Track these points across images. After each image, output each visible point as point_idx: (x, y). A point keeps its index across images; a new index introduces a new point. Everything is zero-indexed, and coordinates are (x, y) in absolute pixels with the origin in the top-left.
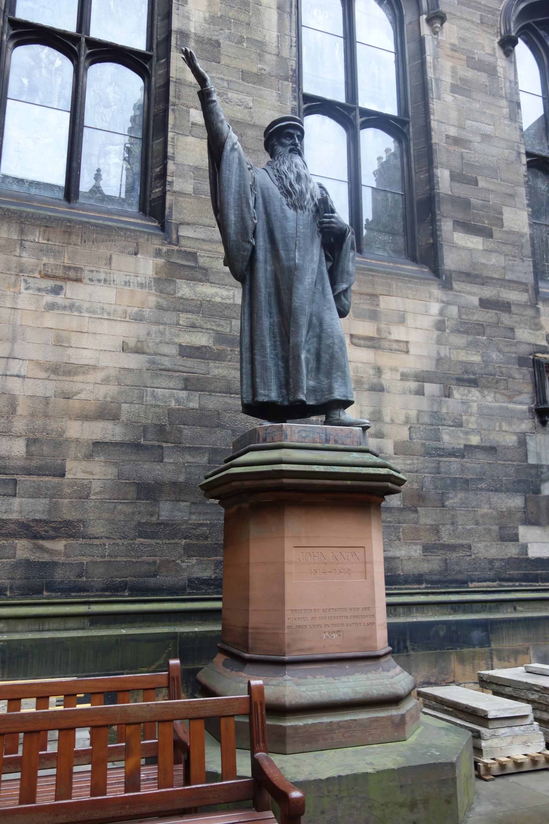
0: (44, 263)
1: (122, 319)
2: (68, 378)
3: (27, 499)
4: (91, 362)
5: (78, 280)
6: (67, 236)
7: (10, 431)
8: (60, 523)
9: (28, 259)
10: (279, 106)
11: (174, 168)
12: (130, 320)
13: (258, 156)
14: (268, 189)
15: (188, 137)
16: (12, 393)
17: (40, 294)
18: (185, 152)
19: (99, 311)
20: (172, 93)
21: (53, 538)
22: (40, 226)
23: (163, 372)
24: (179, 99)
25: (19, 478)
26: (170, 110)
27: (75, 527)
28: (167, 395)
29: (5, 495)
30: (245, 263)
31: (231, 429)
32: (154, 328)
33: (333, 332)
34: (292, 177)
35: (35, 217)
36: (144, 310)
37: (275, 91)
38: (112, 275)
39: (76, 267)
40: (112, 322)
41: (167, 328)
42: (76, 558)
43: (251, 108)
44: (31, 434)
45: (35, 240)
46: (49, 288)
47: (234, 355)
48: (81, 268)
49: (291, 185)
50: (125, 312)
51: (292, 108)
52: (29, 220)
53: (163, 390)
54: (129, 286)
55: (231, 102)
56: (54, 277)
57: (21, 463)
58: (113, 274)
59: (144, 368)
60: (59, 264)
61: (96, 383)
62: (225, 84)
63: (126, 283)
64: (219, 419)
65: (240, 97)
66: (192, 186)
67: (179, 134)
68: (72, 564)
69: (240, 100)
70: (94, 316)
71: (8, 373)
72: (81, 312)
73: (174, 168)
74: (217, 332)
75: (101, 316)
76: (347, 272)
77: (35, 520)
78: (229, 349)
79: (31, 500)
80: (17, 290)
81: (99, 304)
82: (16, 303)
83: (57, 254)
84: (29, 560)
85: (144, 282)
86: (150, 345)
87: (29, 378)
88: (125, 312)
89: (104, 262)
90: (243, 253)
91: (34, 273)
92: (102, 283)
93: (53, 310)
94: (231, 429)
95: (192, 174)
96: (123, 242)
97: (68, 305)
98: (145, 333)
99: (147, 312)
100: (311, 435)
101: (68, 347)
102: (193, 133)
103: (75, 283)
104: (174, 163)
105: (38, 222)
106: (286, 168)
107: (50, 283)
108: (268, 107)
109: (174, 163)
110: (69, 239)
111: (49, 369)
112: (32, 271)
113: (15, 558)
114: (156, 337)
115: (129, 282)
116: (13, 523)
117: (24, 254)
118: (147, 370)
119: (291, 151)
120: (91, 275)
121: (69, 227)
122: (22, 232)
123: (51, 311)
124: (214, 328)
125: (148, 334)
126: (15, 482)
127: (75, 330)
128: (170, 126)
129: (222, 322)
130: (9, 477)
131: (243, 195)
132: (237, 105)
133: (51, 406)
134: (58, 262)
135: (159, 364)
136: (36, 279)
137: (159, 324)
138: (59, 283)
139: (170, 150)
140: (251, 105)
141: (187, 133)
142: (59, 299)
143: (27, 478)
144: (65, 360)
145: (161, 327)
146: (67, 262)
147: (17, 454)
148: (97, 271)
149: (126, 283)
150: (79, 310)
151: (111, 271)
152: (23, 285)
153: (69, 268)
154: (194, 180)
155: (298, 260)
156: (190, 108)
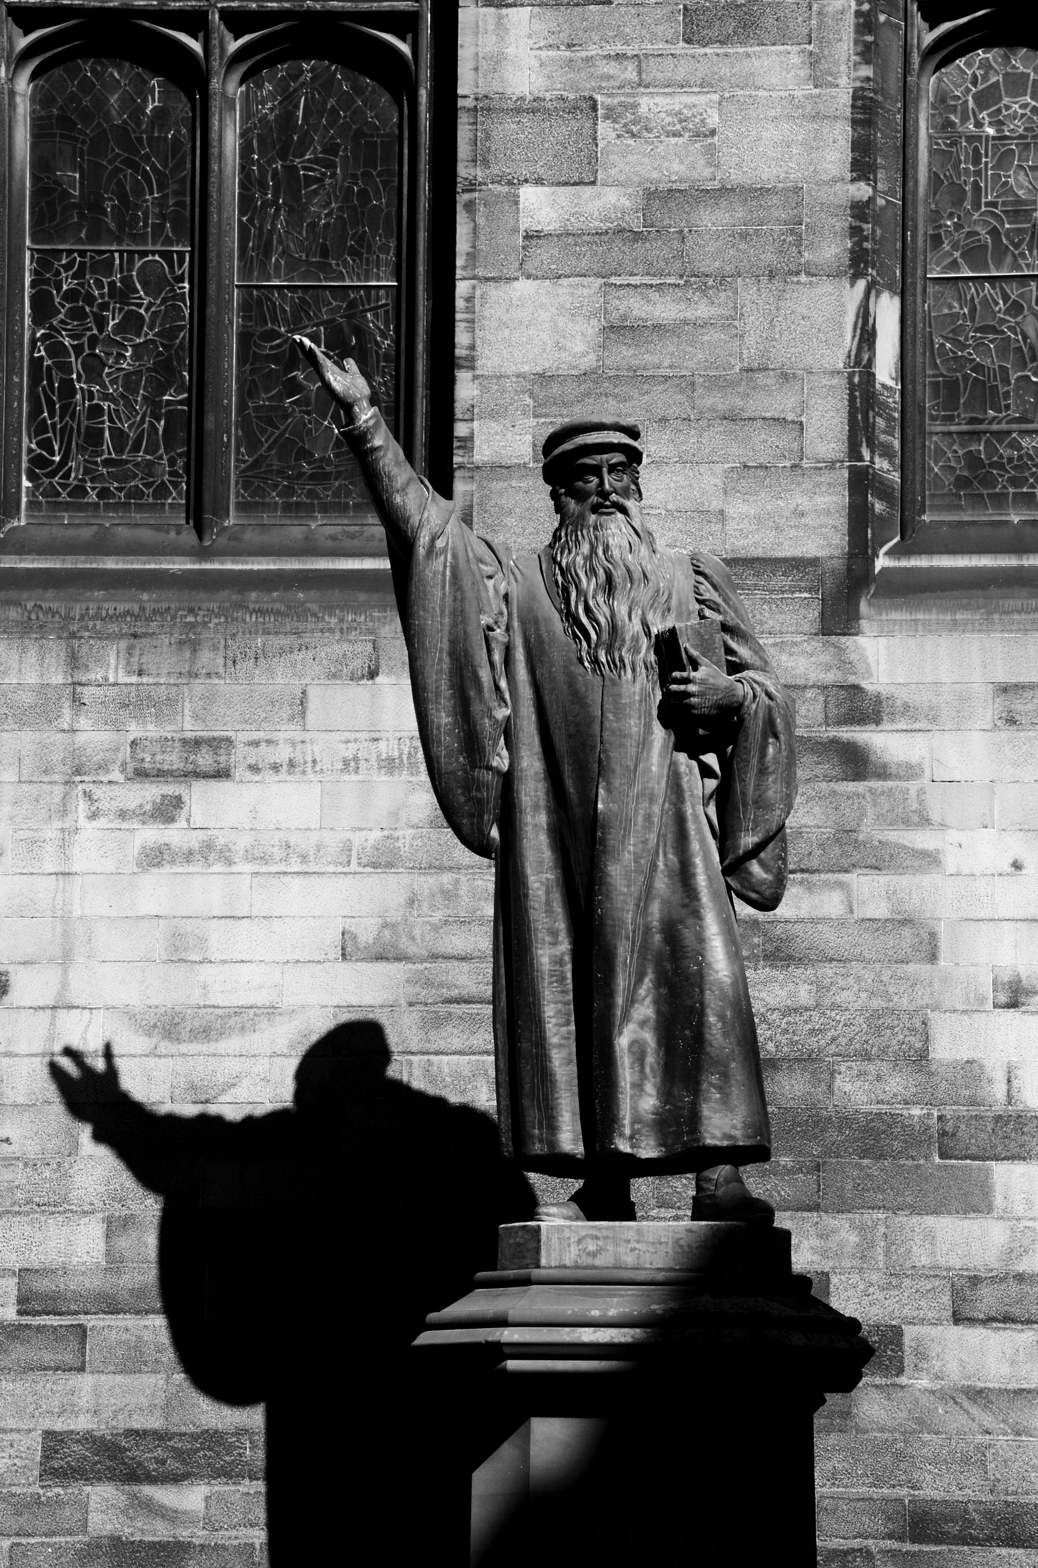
1: (340, 869)
2: (203, 1048)
3: (111, 1376)
4: (261, 998)
5: (222, 774)
6: (188, 655)
7: (65, 1200)
8: (194, 1437)
9: (93, 736)
10: (812, 96)
11: (476, 392)
12: (361, 869)
13: (736, 293)
14: (536, 621)
15: (516, 284)
17: (125, 825)
18: (507, 332)
19: (278, 853)
20: (463, 150)
21: (175, 1479)
22: (121, 636)
23: (454, 1008)
24: (486, 163)
25: (90, 1321)
26: (459, 208)
27: (229, 1448)
28: (466, 1072)
29: (57, 1369)
32: (427, 883)
33: (701, 974)
34: (589, 585)
36: (399, 833)
37: (796, 48)
38: (308, 747)
39: (215, 739)
40: (314, 880)
41: (463, 879)
42: (234, 1533)
43: (713, 133)
44: (117, 1206)
45: (106, 679)
46: (148, 807)
48: (229, 741)
49: (588, 610)
50: (347, 848)
51: (856, 90)
52: (91, 624)
53: (456, 1057)
54: (357, 770)
55: (649, 130)
56: (161, 774)
57: (94, 1283)
58: (312, 742)
59: (403, 1002)
61: (275, 1055)
62: (630, 73)
63: (346, 763)
65: (678, 101)
66: (529, 438)
67: (488, 279)
68: (224, 1548)
69: (680, 113)
70: (265, 869)
72: (230, 863)
73: (476, 392)
75: (282, 867)
77: (130, 1433)
79: (119, 1378)
80: (68, 823)
81: (278, 835)
82: (68, 859)
83: (161, 707)
84: (119, 1538)
85: (396, 754)
86: (417, 932)
88: (347, 848)
89: (286, 712)
90: (479, 795)
91: (108, 771)
92: (283, 774)
93: (159, 865)
95: (529, 401)
96: (336, 647)
97: (196, 846)
98: (402, 899)
99: (406, 837)
100: (610, 1247)
102: (528, 266)
103: (214, 785)
104: (475, 378)
105: (113, 628)
106: (580, 560)
107: (151, 792)
108: (772, 113)
109: (475, 378)
110: (193, 660)
111: (155, 1026)
112: (103, 767)
113: (85, 1532)
114: (433, 907)
115: (356, 759)
116: (78, 1441)
117: (83, 723)
118: (411, 1004)
120: (252, 756)
121: (193, 625)
122: (74, 661)
123: (155, 870)
125: (411, 902)
126: (82, 1331)
128: (460, 262)
130: (67, 1321)
131: (463, 659)
134: (168, 731)
135: (441, 985)
136: (113, 787)
137: (441, 869)
138: (171, 789)
139: (462, 338)
140: (714, 120)
141: (512, 269)
142: (174, 835)
143: (110, 1320)
144: (196, 997)
145: (447, 878)
146: (191, 728)
147: (85, 1258)
148: (269, 742)
149: (346, 763)
150: (226, 859)
151: (307, 736)
152: (82, 807)
153: (197, 743)
154: (535, 416)
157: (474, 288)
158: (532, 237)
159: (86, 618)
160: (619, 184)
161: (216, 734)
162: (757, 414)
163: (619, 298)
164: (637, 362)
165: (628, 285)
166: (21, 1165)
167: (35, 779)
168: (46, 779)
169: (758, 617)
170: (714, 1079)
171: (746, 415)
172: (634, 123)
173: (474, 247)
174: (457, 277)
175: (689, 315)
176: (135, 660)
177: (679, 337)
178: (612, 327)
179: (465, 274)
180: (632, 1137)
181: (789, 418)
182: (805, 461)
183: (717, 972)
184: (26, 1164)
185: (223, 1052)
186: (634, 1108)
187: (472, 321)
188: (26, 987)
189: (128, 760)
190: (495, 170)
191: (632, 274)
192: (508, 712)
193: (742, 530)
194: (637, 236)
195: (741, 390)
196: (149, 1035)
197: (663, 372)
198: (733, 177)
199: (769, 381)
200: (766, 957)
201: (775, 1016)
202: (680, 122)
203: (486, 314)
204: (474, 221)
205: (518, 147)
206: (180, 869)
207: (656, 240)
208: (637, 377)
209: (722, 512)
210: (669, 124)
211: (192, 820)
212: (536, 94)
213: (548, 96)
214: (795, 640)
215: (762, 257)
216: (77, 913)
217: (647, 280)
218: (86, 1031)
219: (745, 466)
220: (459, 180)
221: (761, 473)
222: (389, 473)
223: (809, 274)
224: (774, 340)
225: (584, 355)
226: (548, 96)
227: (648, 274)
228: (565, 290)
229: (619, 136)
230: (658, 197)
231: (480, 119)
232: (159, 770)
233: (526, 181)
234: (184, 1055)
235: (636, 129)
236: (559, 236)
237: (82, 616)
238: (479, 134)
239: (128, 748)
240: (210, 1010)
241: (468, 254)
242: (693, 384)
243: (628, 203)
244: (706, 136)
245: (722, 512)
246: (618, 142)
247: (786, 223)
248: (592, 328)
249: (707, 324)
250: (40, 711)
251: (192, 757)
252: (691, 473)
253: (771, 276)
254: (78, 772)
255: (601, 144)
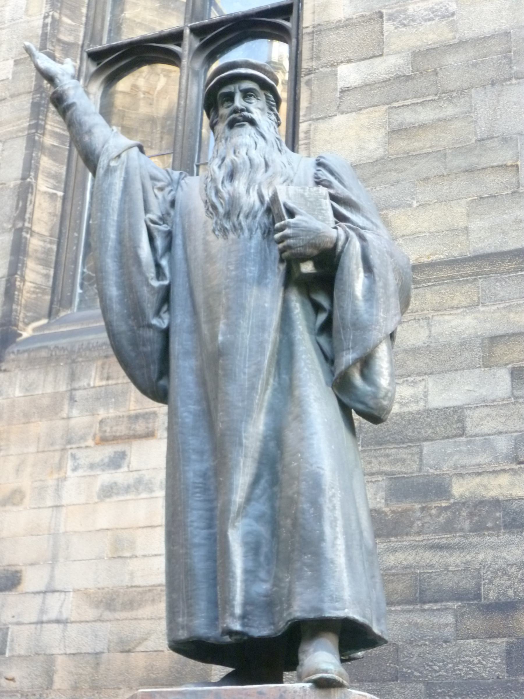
0: (100, 418)
13: (471, 97)
15: (335, 118)
16: (48, 652)
17: (93, 473)
18: (329, 146)
30: (152, 367)
31: (423, 682)
35: (91, 345)
43: (453, 14)
45: (89, 384)
46: (106, 460)
47: (427, 519)
49: (217, 192)
52: (83, 354)
55: (414, 21)
60: (121, 414)
64: (397, 661)
67: (318, 119)
69: (432, 8)
71: (45, 618)
72: (151, 491)
74: (391, 476)
76: (354, 325)
78: (417, 506)
80: (62, 474)
87: (72, 622)
90: (145, 349)
93: (110, 496)
94: (423, 682)
97: (131, 481)
101: (131, 557)
102: (343, 108)
105: (96, 354)
107: (108, 451)
111: (101, 601)
112: (83, 438)
117: (75, 412)
119: (232, 125)
122: (73, 377)
123: (108, 500)
124: (387, 468)
127: (141, 524)
128: (302, 112)
129: (403, 454)
132: (426, 21)
133: (102, 667)
134: (122, 412)
136: (88, 450)
138: (119, 448)
142: (120, 476)
144: (126, 581)
152: (70, 464)
153: (137, 417)
155: (224, 335)
156: (338, 64)
157: (310, 125)
158: (345, 91)
159: (81, 350)
160: (397, 53)
161: (147, 410)
162: (488, 165)
163: (397, 114)
164: (409, 148)
165: (403, 106)
166: (19, 695)
167: (46, 449)
168: (52, 448)
169: (493, 291)
170: (307, 558)
171: (480, 167)
172: (405, 19)
173: (310, 103)
174: (301, 121)
175: (441, 115)
176: (106, 371)
177: (435, 129)
178: (394, 131)
179: (305, 119)
180: (244, 617)
181: (509, 164)
182: (521, 188)
183: (311, 465)
184: (22, 695)
185: (140, 617)
186: (246, 592)
187: (308, 144)
188: (33, 580)
189: (97, 432)
190: (324, 60)
191: (405, 99)
192: (166, 282)
193: (480, 237)
194: (408, 78)
195: (476, 152)
196: (97, 607)
197: (425, 151)
198: (466, 35)
199: (495, 144)
200: (506, 527)
201: (514, 569)
202: (433, 13)
203: (317, 138)
204: (311, 89)
205: (337, 46)
206: (121, 498)
207: (420, 78)
208: (409, 156)
209: (466, 228)
210: (426, 15)
211: (131, 466)
212: (348, 17)
213: (354, 16)
214: (519, 303)
215: (487, 75)
216: (62, 530)
217: (415, 101)
218: (61, 607)
219: (481, 198)
220: (303, 70)
221: (491, 200)
222: (80, 120)
223: (517, 78)
224: (498, 120)
225: (376, 150)
226: (354, 16)
227: (415, 97)
228: (364, 116)
229: (396, 28)
230: (420, 55)
231: (315, 36)
232: (114, 436)
233: (342, 62)
234: (118, 620)
235: (405, 21)
236: (361, 87)
237: (79, 349)
238: (315, 44)
239: (98, 425)
240: (134, 589)
241: (307, 108)
242: (445, 155)
243: (402, 62)
244: (449, 17)
245: (466, 228)
246: (396, 31)
247: (501, 53)
248: (381, 134)
249: (454, 118)
250: (53, 409)
251: (133, 426)
252: (445, 208)
253: (493, 84)
254: (69, 442)
255: (386, 34)
